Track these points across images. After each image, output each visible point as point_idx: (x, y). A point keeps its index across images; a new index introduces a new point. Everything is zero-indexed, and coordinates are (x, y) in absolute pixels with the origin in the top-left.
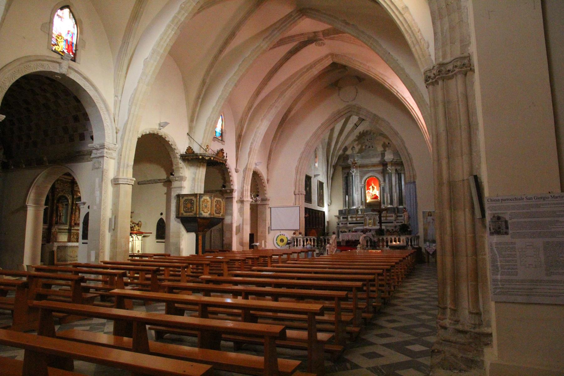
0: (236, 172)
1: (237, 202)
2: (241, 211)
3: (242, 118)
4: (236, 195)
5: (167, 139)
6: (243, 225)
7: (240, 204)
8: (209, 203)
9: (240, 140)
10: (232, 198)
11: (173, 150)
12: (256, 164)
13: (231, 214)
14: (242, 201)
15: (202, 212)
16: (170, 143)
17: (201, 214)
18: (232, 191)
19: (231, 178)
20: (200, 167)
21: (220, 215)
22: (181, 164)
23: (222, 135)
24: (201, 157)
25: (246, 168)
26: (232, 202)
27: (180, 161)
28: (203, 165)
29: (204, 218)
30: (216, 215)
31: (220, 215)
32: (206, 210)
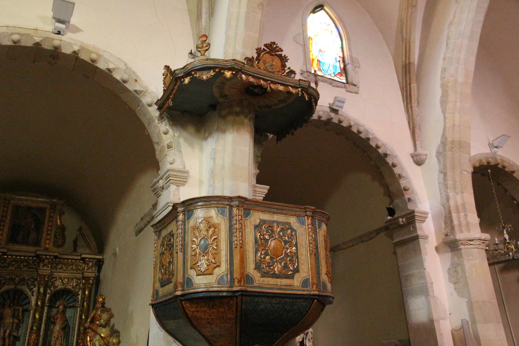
0: (419, 163)
1: (437, 249)
2: (457, 276)
3: (401, 21)
4: (429, 229)
5: (102, 65)
6: (474, 322)
7: (448, 255)
8: (223, 235)
9: (409, 78)
10: (417, 238)
11: (135, 97)
12: (491, 146)
13: (425, 291)
14: (451, 245)
15: (192, 273)
16: (118, 76)
17: (189, 282)
18: (411, 218)
19: (403, 183)
20: (224, 131)
21: (297, 282)
22: (164, 133)
23: (344, 71)
24: (187, 80)
25: (444, 143)
26: (417, 251)
27: (164, 126)
28: (237, 125)
29: (209, 299)
30: (261, 283)
31: (297, 282)
32: (203, 263)
